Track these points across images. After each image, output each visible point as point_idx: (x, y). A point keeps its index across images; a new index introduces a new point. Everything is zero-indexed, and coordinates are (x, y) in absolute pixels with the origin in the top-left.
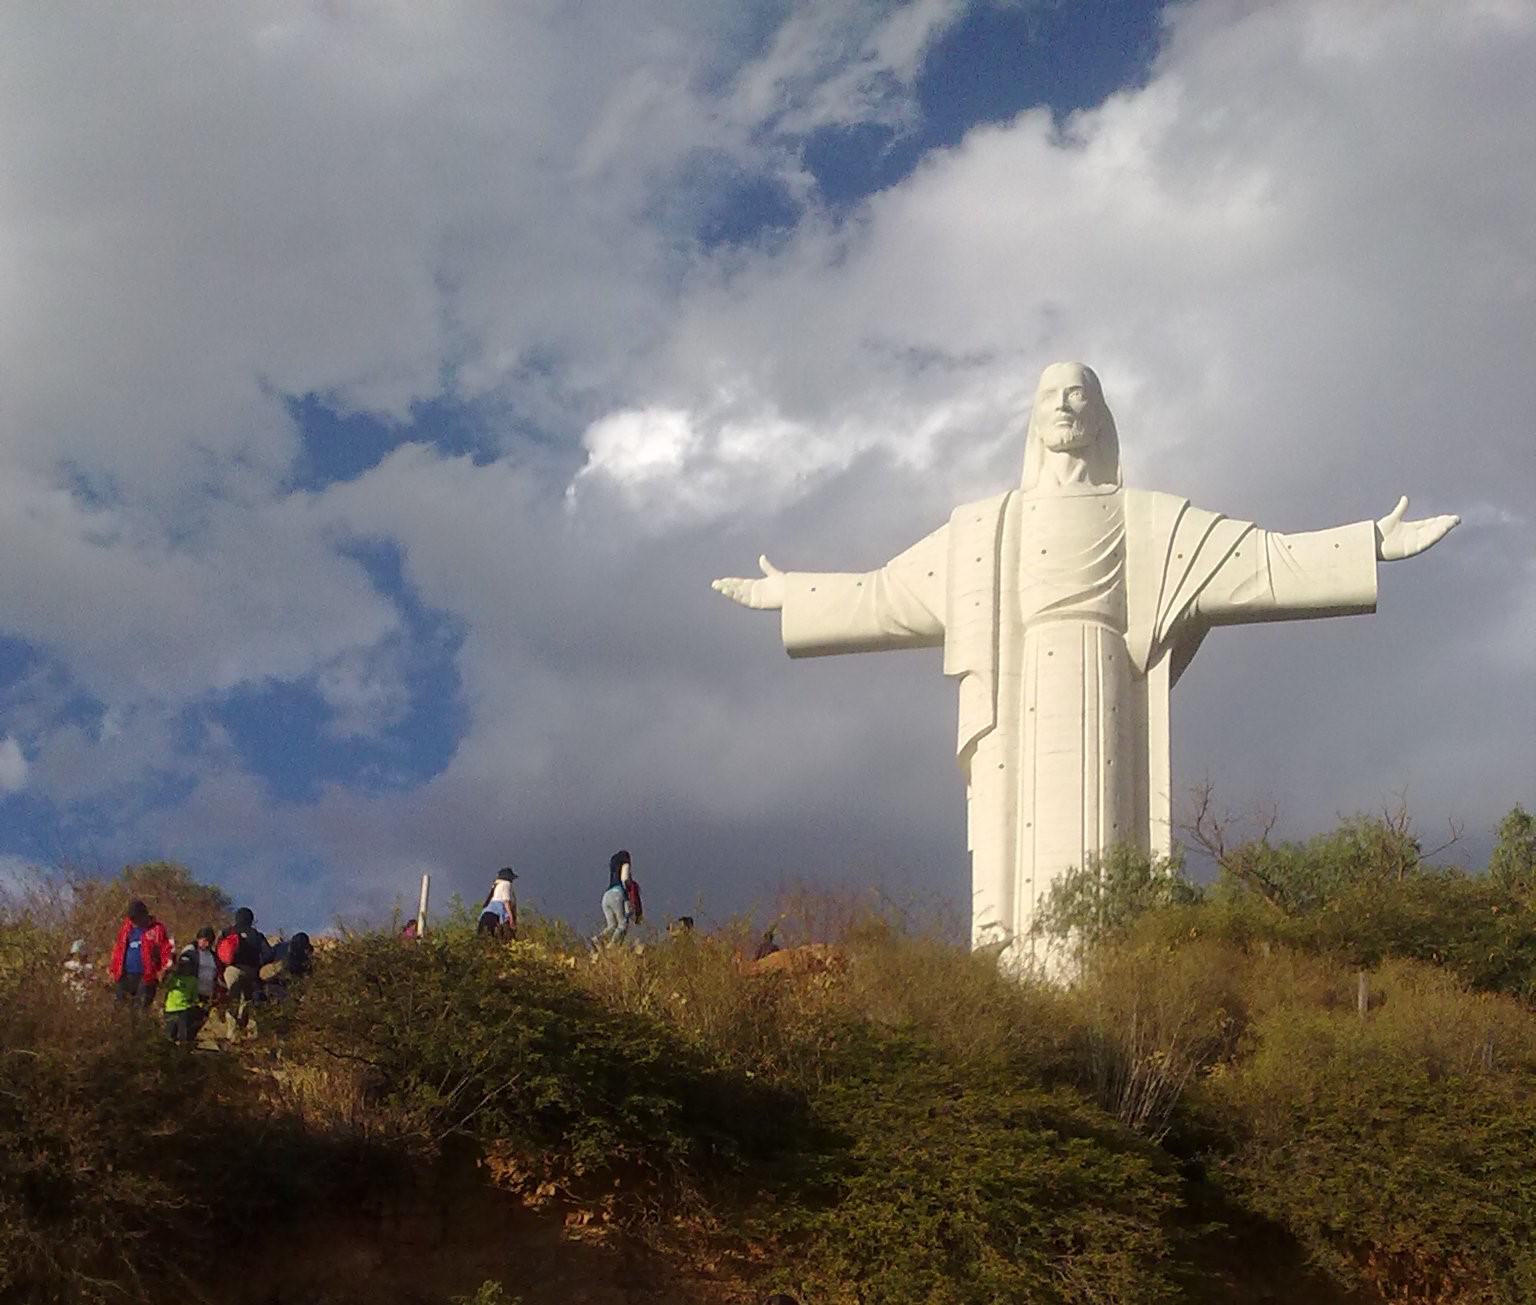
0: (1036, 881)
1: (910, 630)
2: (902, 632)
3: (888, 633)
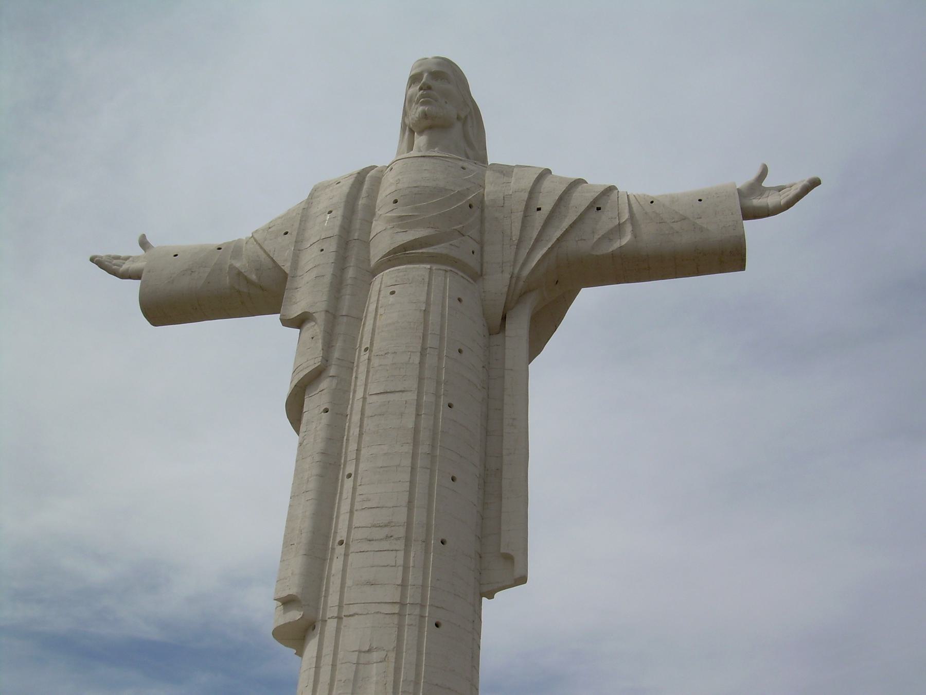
1: (262, 288)
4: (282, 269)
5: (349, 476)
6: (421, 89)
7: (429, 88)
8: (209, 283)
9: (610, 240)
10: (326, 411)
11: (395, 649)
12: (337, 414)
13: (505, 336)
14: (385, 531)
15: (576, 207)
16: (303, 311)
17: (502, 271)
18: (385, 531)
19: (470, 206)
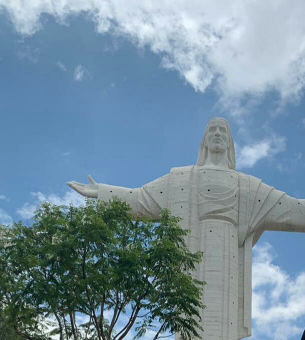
1: (151, 214)
2: (147, 214)
6: (216, 135)
7: (219, 136)
9: (283, 217)
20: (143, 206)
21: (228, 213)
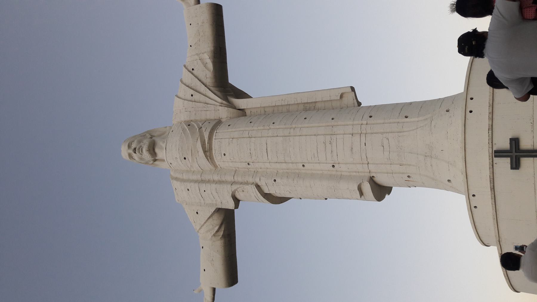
0: (333, 162)
2: (223, 229)
3: (223, 235)
4: (213, 213)
5: (303, 166)
6: (135, 153)
7: (135, 149)
8: (218, 251)
10: (275, 181)
11: (382, 134)
12: (276, 176)
13: (247, 108)
14: (328, 146)
15: (192, 79)
16: (231, 198)
17: (219, 110)
18: (328, 146)
19: (189, 125)
20: (214, 235)
21: (205, 135)
